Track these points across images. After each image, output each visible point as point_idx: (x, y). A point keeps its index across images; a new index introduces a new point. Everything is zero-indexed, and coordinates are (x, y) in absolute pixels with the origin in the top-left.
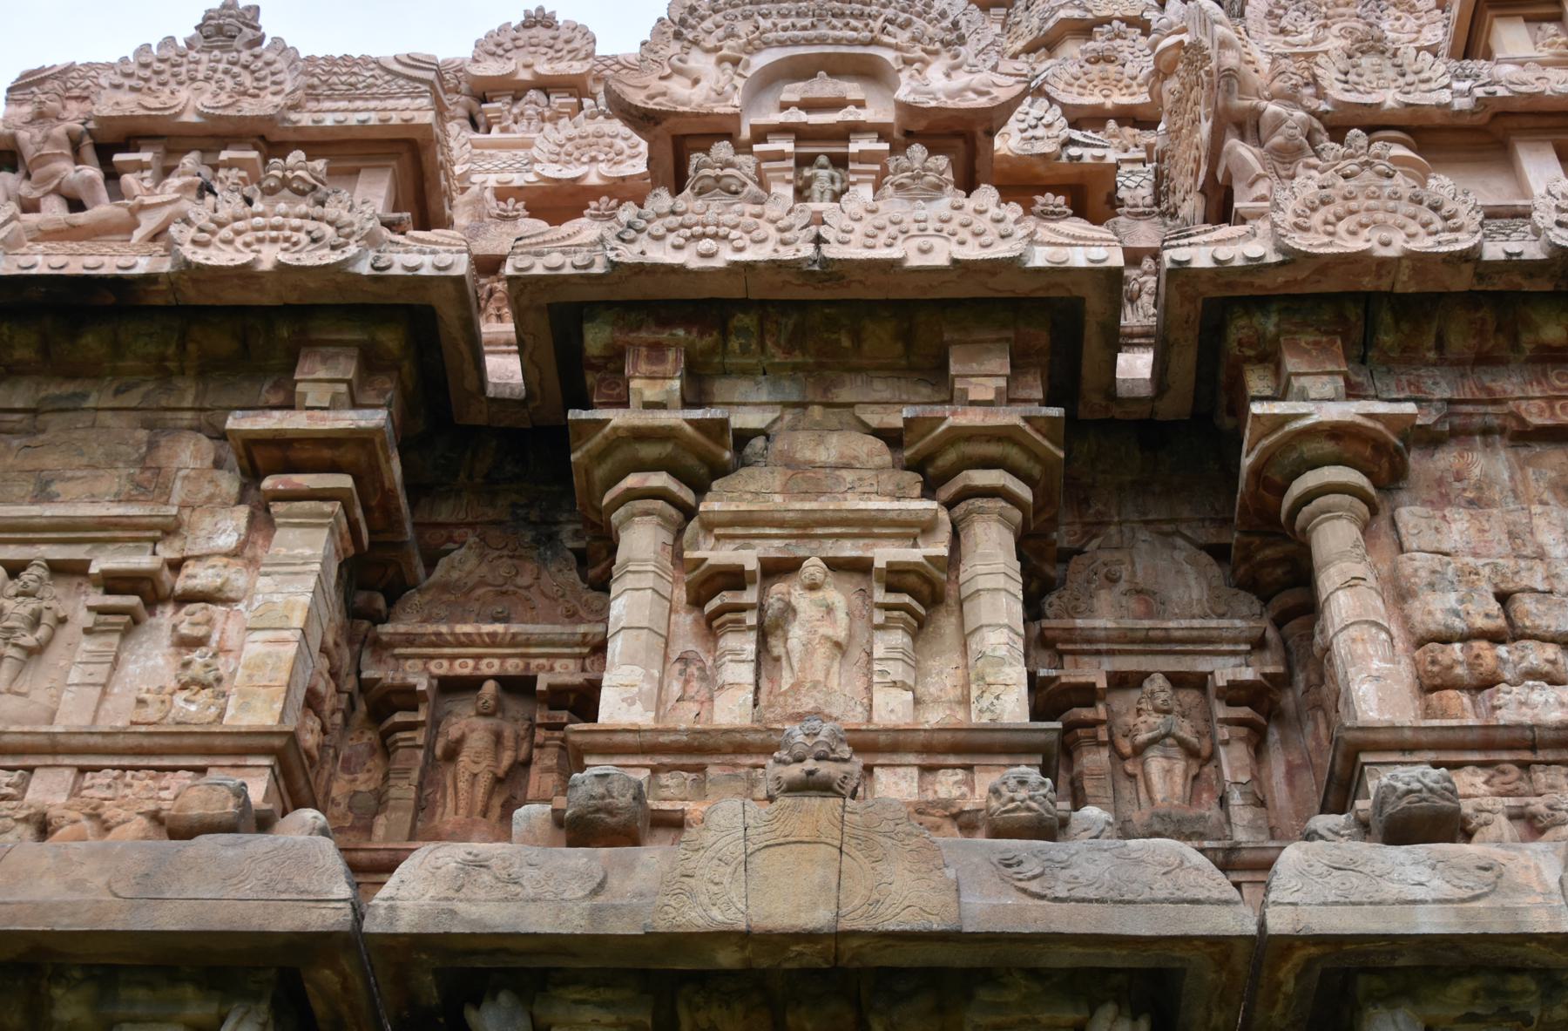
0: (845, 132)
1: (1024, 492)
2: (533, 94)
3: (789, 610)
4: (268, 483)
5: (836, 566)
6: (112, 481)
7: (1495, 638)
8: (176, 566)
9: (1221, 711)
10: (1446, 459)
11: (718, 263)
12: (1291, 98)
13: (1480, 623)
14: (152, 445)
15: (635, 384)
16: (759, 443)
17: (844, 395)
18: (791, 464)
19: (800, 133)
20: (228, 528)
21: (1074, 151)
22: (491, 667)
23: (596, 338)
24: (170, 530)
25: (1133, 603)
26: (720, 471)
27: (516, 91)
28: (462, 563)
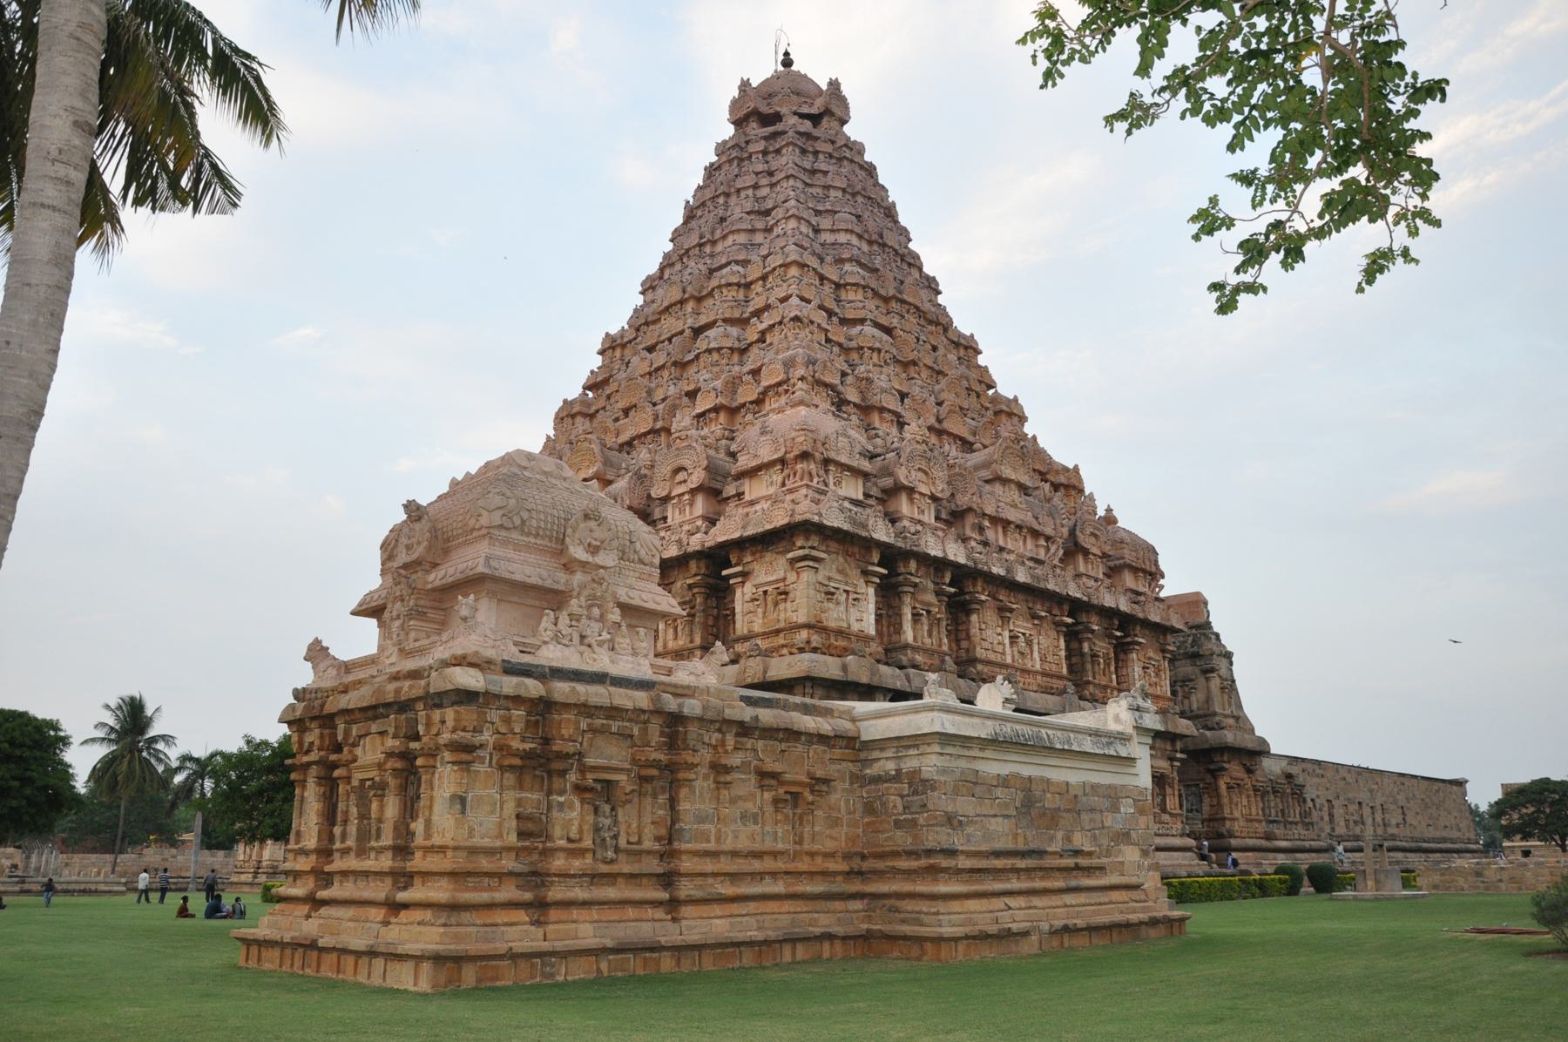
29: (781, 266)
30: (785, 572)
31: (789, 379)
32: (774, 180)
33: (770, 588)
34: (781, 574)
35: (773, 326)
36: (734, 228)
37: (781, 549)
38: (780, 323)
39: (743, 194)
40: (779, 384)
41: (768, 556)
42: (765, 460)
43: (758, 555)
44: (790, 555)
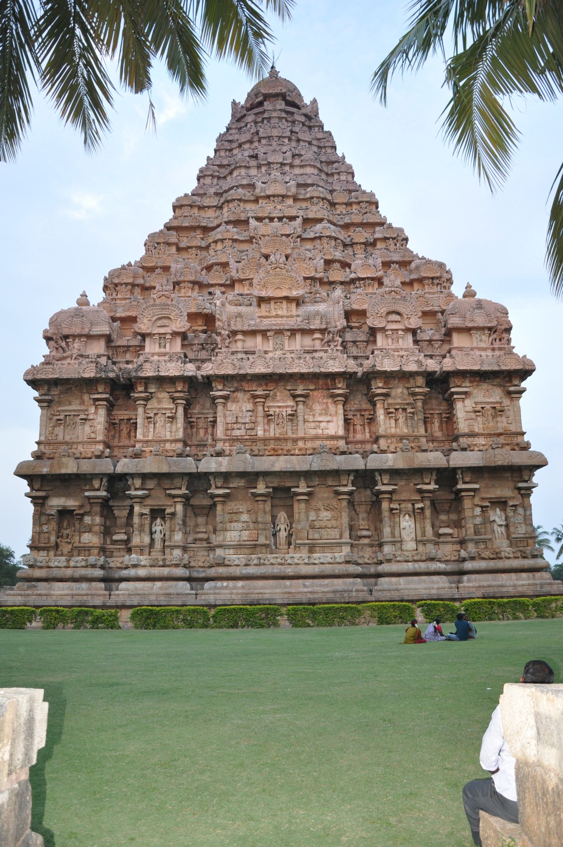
0: (165, 334)
1: (184, 402)
2: (124, 286)
3: (157, 421)
4: (96, 404)
5: (163, 414)
6: (78, 402)
7: (234, 423)
8: (88, 415)
9: (209, 424)
10: (235, 394)
11: (146, 375)
12: (225, 330)
13: (233, 422)
14: (82, 396)
15: (138, 388)
16: (153, 394)
17: (164, 386)
18: (157, 398)
19: (160, 334)
20: (92, 410)
21: (205, 311)
22: (125, 417)
23: (133, 380)
24: (86, 410)
25: (201, 407)
26: (150, 399)
27: (122, 285)
28: (120, 402)
29: (367, 202)
30: (501, 398)
31: (441, 277)
32: (322, 145)
33: (488, 407)
34: (498, 399)
35: (388, 238)
36: (312, 163)
37: (495, 383)
38: (394, 239)
39: (302, 143)
40: (433, 278)
41: (485, 386)
42: (481, 325)
43: (475, 383)
44: (512, 389)
